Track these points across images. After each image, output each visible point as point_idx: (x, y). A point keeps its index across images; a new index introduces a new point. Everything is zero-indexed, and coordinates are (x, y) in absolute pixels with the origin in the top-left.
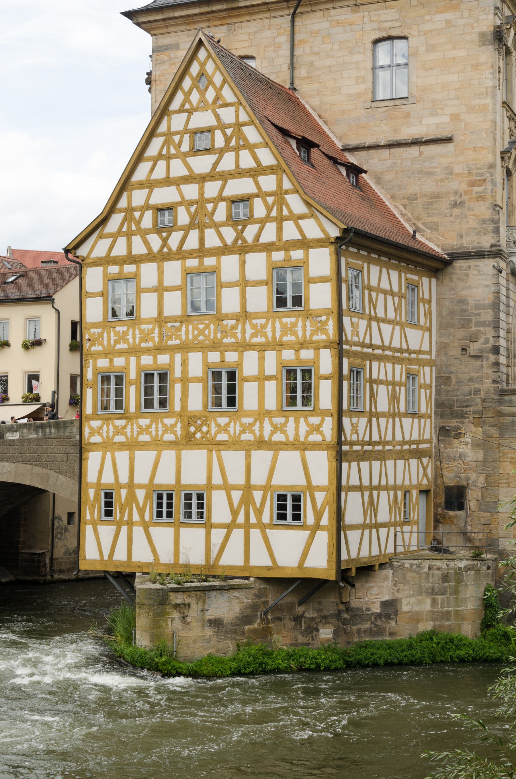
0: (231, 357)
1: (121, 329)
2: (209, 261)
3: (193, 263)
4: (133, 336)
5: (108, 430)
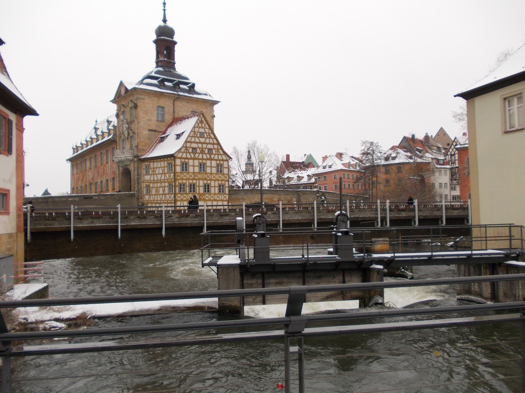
0: (209, 182)
1: (185, 174)
2: (204, 161)
3: (201, 161)
4: (188, 176)
5: (182, 197)
